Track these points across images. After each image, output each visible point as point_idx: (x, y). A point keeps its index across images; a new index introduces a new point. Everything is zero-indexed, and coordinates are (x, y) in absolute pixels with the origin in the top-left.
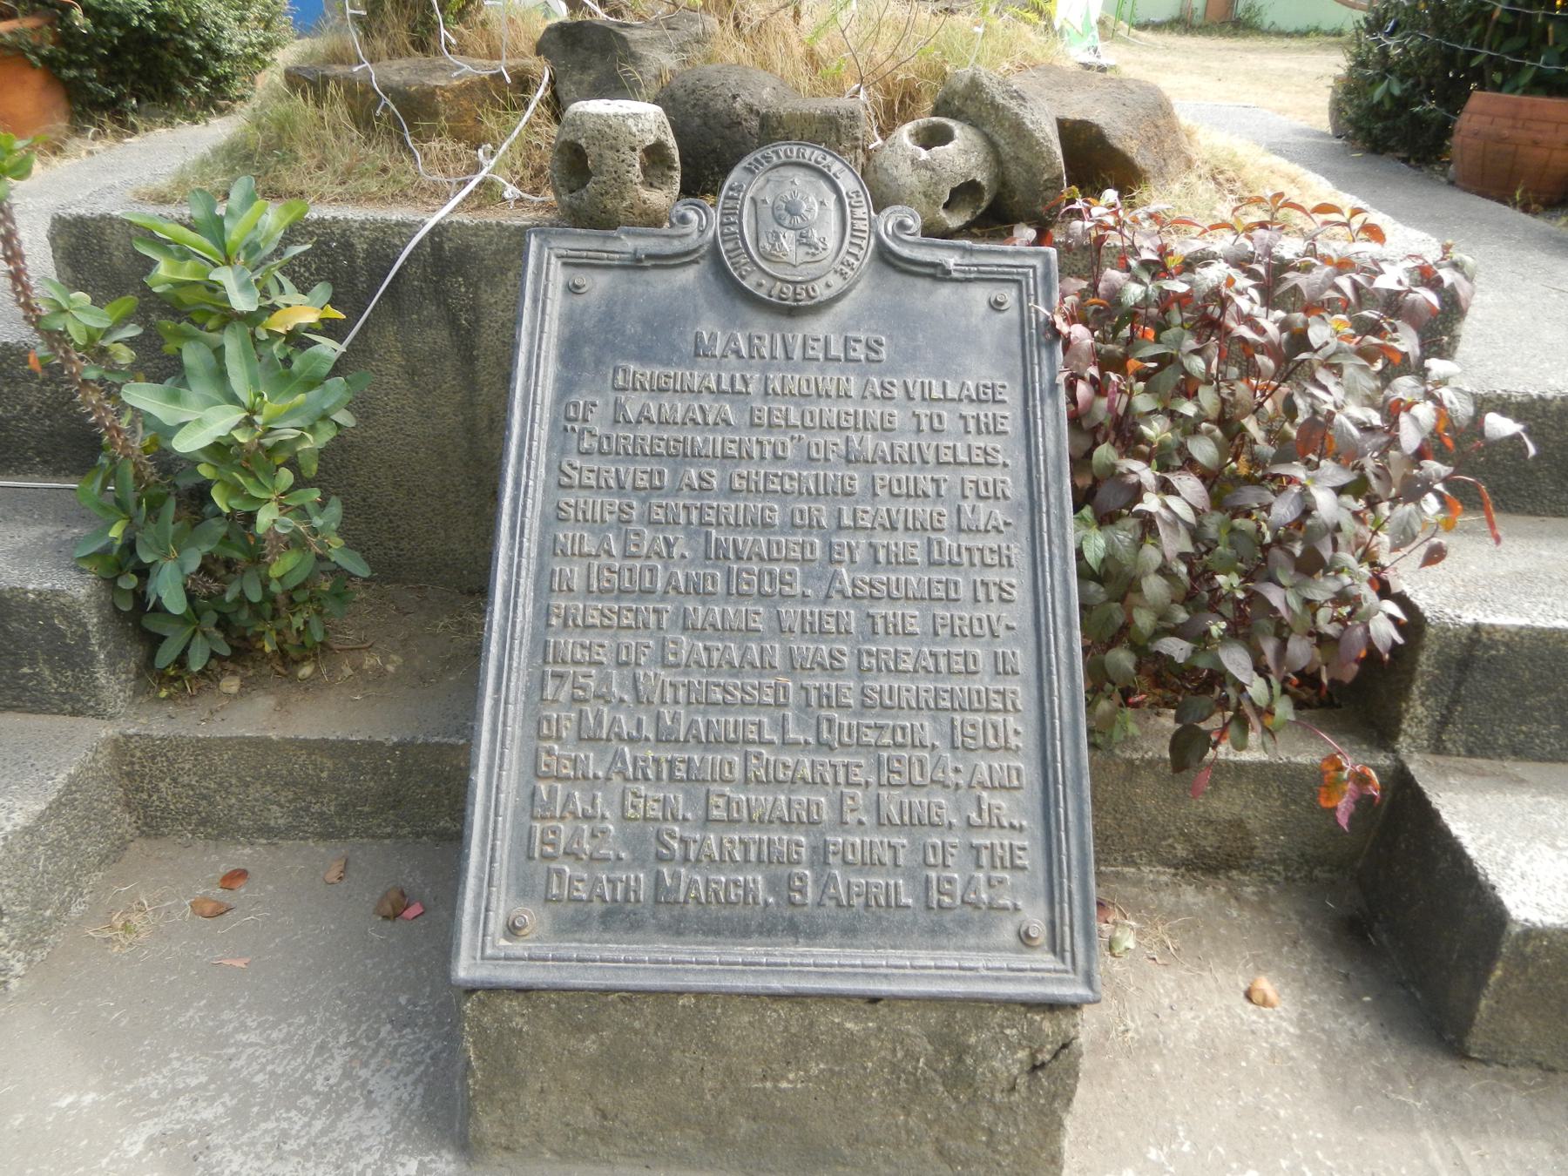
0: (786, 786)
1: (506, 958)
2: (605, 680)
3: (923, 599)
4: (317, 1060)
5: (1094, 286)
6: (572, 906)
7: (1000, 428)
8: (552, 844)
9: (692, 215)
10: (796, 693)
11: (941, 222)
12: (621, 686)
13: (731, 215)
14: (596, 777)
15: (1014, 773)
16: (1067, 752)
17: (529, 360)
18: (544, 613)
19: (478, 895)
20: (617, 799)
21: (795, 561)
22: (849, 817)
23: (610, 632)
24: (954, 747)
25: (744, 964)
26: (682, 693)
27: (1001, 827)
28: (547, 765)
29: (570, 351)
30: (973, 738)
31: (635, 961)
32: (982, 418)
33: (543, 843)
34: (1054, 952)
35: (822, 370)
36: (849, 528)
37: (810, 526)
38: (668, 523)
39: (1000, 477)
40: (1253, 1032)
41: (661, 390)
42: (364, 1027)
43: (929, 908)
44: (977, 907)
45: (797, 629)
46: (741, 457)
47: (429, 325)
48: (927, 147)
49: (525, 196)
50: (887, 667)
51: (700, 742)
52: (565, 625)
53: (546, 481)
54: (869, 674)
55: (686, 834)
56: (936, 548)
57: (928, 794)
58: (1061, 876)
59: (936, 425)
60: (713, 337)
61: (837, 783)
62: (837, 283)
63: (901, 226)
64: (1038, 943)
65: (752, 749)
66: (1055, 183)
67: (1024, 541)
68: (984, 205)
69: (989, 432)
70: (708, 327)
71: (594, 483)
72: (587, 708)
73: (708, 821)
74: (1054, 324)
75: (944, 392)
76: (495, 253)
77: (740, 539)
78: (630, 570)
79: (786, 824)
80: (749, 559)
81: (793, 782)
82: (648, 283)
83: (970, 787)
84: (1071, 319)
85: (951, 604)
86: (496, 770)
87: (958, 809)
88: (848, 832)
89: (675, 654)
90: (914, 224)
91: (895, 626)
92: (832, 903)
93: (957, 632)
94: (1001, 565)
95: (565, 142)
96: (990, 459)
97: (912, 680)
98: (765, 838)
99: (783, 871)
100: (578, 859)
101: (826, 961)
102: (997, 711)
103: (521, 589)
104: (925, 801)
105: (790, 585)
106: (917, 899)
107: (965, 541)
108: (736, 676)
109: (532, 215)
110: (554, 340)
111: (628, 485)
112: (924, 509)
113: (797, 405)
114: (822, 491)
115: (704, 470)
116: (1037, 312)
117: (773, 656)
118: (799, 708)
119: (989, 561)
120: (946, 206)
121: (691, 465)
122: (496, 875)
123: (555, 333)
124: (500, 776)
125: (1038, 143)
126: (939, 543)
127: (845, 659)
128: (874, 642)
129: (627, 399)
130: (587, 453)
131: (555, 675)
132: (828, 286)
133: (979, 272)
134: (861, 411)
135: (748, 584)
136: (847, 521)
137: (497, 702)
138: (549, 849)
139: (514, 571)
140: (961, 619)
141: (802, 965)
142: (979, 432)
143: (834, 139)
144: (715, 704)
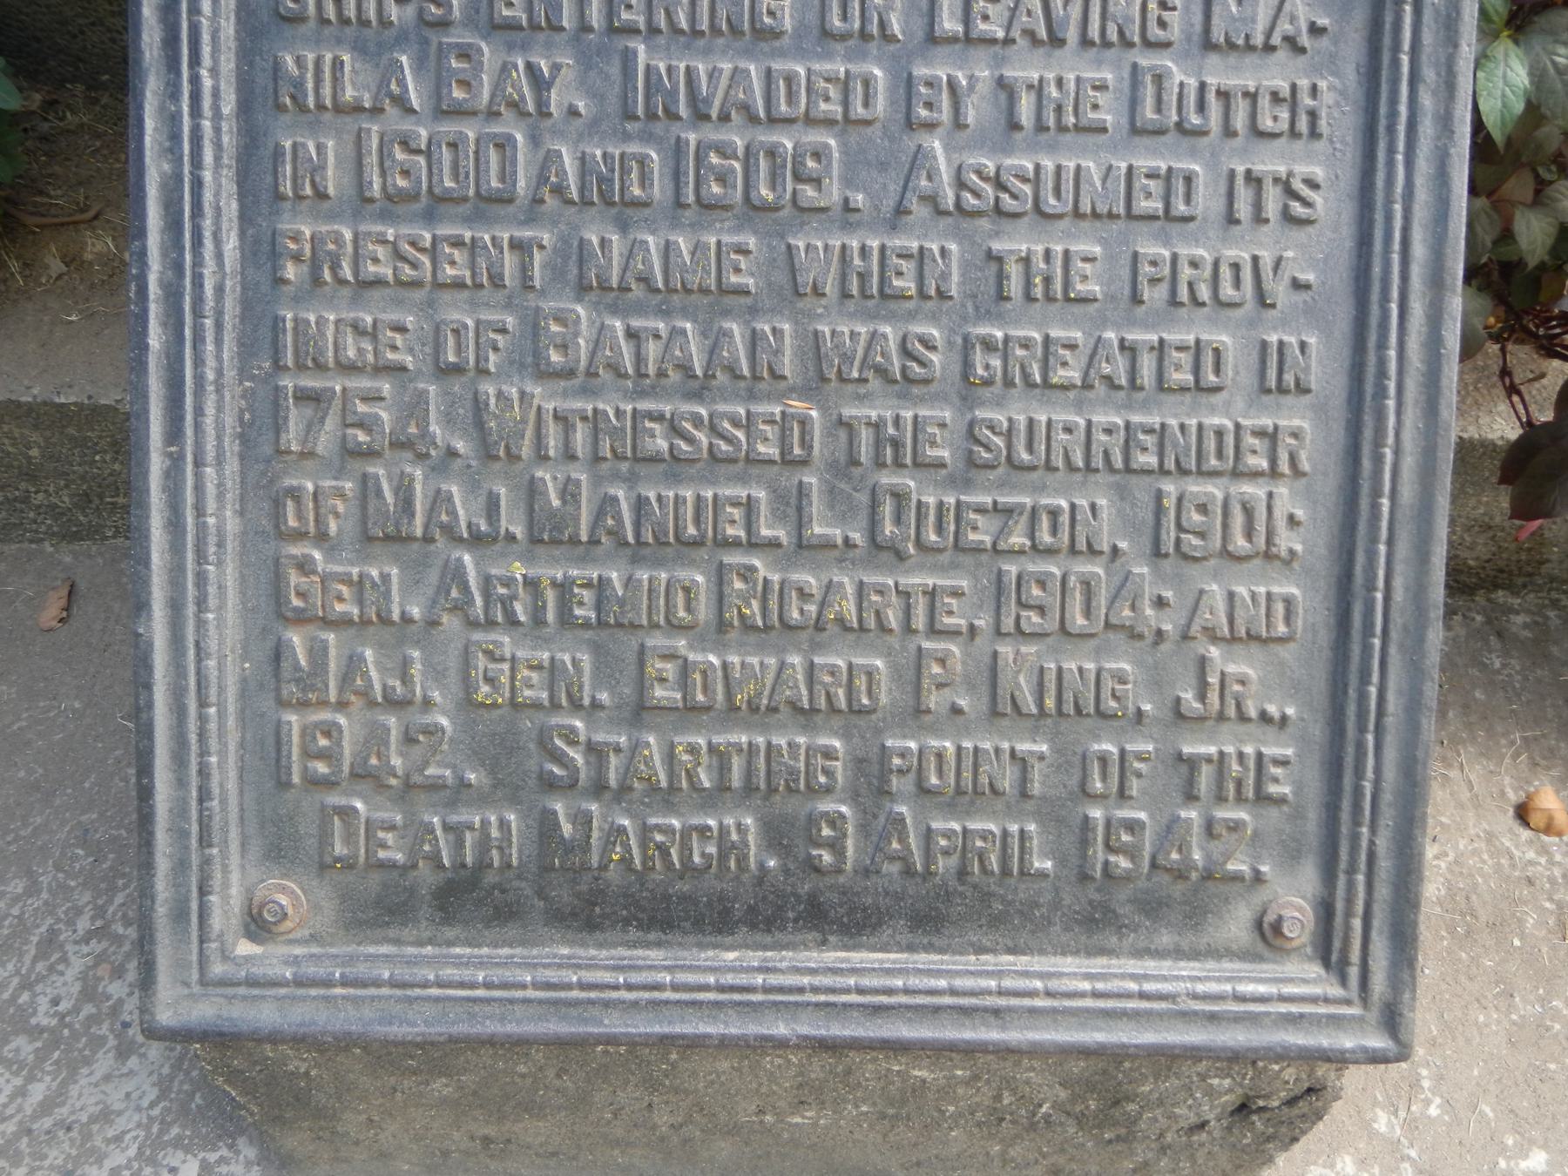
0: (804, 636)
1: (252, 982)
2: (415, 408)
3: (1111, 216)
4: (41, 967)
6: (375, 879)
8: (322, 755)
10: (829, 434)
12: (449, 420)
14: (406, 619)
15: (1279, 608)
16: (1399, 567)
18: (263, 251)
19: (181, 866)
20: (453, 662)
21: (829, 122)
22: (933, 700)
23: (418, 295)
24: (1157, 553)
25: (722, 989)
26: (580, 435)
27: (1243, 718)
28: (300, 594)
30: (1202, 535)
33: (307, 754)
34: (1326, 963)
36: (953, 40)
38: (535, 27)
40: (1530, 882)
42: (119, 899)
43: (1084, 878)
45: (830, 288)
50: (1026, 376)
52: (317, 281)
54: (986, 393)
55: (599, 737)
56: (1149, 91)
61: (908, 629)
64: (1295, 944)
65: (734, 558)
67: (1351, 76)
72: (378, 470)
73: (640, 711)
78: (453, 146)
79: (805, 715)
80: (725, 118)
85: (1175, 228)
86: (191, 609)
87: (1156, 681)
88: (935, 730)
89: (563, 347)
91: (1047, 280)
93: (1183, 293)
94: (1294, 133)
97: (1079, 406)
100: (382, 787)
102: (1255, 475)
103: (208, 196)
104: (1090, 666)
105: (817, 182)
106: (1061, 862)
107: (1219, 74)
108: (697, 396)
117: (778, 352)
119: (1267, 124)
124: (201, 624)
126: (1159, 79)
127: (934, 358)
131: (303, 396)
135: (722, 179)
137: (176, 461)
138: (322, 768)
140: (1194, 264)
141: (833, 991)
144: (655, 459)
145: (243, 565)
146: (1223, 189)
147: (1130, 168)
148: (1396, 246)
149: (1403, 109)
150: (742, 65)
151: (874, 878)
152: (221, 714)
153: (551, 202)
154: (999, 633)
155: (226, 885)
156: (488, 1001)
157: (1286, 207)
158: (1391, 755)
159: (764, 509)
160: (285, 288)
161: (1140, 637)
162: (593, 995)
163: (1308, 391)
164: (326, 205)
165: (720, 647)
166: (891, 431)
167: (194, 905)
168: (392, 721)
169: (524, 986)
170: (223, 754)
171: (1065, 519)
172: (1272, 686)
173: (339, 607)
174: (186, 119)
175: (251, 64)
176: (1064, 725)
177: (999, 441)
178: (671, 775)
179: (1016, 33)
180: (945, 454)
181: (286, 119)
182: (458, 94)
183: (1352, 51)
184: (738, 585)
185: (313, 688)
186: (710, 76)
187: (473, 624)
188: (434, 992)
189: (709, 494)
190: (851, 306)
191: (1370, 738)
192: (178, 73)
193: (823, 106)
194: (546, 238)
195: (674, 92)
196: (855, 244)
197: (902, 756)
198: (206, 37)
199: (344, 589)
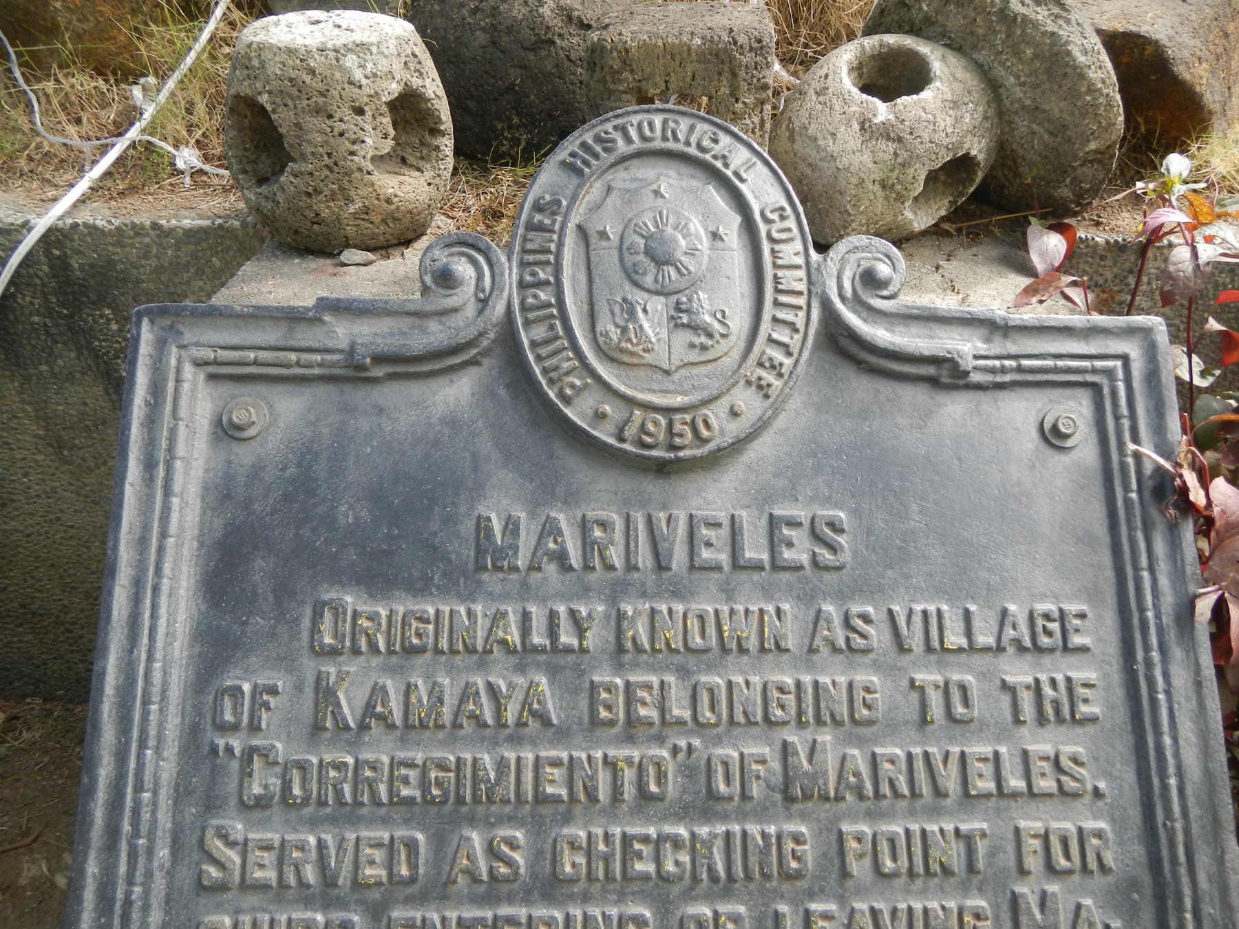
7: (1084, 709)
13: (538, 260)
17: (136, 600)
29: (223, 575)
32: (1048, 691)
35: (729, 593)
39: (1090, 825)
41: (411, 651)
47: (70, 378)
49: (207, 167)
59: (959, 709)
60: (511, 527)
69: (1060, 720)
71: (270, 875)
74: (1184, 490)
75: (969, 633)
76: (159, 270)
95: (237, 96)
111: (344, 879)
113: (683, 672)
114: (739, 872)
115: (504, 832)
116: (1137, 456)
121: (472, 821)
123: (192, 531)
129: (341, 677)
132: (734, 414)
133: (1020, 369)
142: (1041, 719)
143: (725, 90)
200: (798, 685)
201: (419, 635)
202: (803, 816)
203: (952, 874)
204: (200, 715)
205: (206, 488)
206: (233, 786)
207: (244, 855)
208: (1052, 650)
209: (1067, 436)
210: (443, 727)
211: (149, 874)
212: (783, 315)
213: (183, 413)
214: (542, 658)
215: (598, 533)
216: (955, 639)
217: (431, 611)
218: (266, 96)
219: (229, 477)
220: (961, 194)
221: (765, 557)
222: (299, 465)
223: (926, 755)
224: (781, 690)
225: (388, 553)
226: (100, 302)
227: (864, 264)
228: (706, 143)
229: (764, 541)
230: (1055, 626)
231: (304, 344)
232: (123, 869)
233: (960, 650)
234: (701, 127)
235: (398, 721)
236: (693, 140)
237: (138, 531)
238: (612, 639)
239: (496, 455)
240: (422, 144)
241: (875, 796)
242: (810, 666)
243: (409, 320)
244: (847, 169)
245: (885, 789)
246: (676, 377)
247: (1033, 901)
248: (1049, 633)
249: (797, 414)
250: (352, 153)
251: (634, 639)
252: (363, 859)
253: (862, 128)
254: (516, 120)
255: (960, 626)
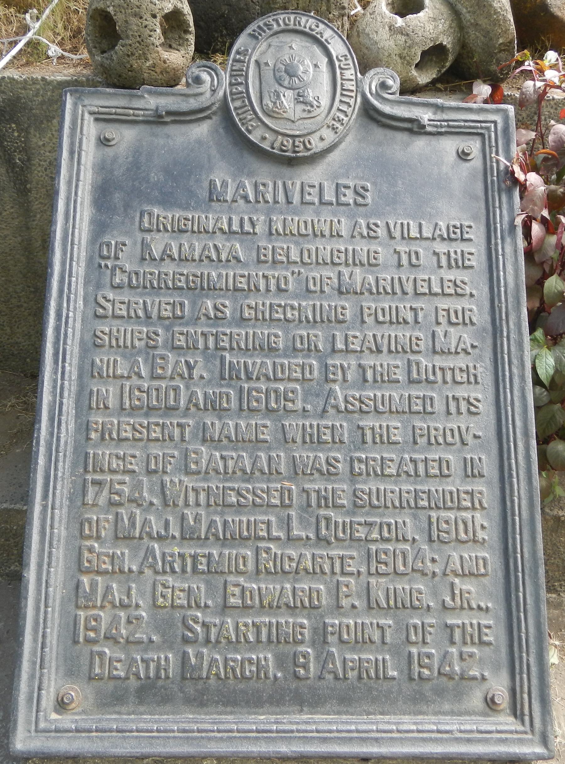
0: (291, 576)
1: (57, 731)
2: (138, 486)
3: (403, 412)
5: (542, 137)
6: (111, 685)
7: (467, 263)
8: (94, 629)
9: (205, 77)
10: (299, 495)
11: (412, 80)
12: (151, 491)
13: (239, 76)
14: (130, 571)
15: (481, 562)
16: (525, 544)
17: (67, 205)
18: (84, 428)
19: (32, 677)
20: (149, 589)
21: (297, 380)
22: (344, 602)
23: (141, 444)
24: (431, 540)
25: (258, 731)
26: (202, 497)
27: (471, 608)
28: (88, 561)
30: (447, 533)
31: (165, 731)
32: (452, 255)
33: (87, 629)
34: (515, 716)
35: (318, 213)
36: (342, 351)
37: (309, 350)
38: (188, 348)
39: (467, 306)
43: (411, 679)
44: (451, 678)
45: (299, 439)
46: (250, 290)
48: (402, 15)
49: (66, 54)
50: (375, 472)
51: (218, 539)
52: (103, 438)
53: (84, 312)
54: (360, 478)
55: (207, 620)
56: (414, 368)
57: (410, 581)
58: (521, 651)
59: (414, 261)
60: (224, 184)
61: (333, 573)
62: (329, 137)
63: (383, 86)
64: (501, 707)
65: (262, 544)
66: (507, 48)
68: (448, 64)
69: (458, 267)
70: (220, 175)
71: (125, 313)
72: (122, 510)
73: (225, 608)
74: (513, 173)
75: (420, 232)
76: (43, 103)
77: (250, 362)
78: (157, 390)
79: (292, 609)
80: (258, 379)
81: (297, 572)
82: (168, 136)
83: (445, 574)
84: (526, 169)
85: (427, 417)
86: (45, 567)
87: (435, 594)
88: (344, 615)
89: (197, 463)
90: (394, 84)
92: (330, 677)
94: (469, 382)
95: (96, 10)
96: (459, 291)
97: (396, 483)
98: (274, 621)
99: (289, 649)
100: (117, 642)
101: (326, 727)
102: (466, 509)
103: (65, 408)
104: (407, 587)
105: (293, 401)
106: (401, 672)
107: (439, 361)
108: (248, 481)
109: (72, 71)
110: (88, 188)
111: (154, 315)
112: (404, 334)
113: (297, 243)
114: (318, 319)
115: (219, 301)
116: (498, 162)
117: (279, 464)
118: (301, 508)
119: (459, 379)
120: (417, 66)
121: (207, 297)
122: (47, 659)
124: (48, 572)
125: (496, 13)
126: (418, 364)
127: (339, 465)
128: (364, 450)
130: (119, 287)
131: (94, 482)
132: (322, 139)
133: (449, 126)
134: (350, 248)
135: (257, 401)
136: (340, 345)
137: (45, 507)
138: (92, 634)
139: (58, 392)
140: (436, 429)
141: (306, 731)
142: (450, 267)
143: (324, 8)
144: (231, 506)
145: (67, 549)
146: (445, 402)
147: (409, 395)
148: (510, 422)
149: (507, 374)
150: (265, 360)
151: (323, 681)
152: (53, 611)
153: (193, 409)
154: (369, 574)
155: (49, 687)
156: (158, 738)
157: (469, 409)
158: (531, 621)
159: (274, 525)
160: (91, 442)
161: (426, 575)
162: (203, 735)
163: (483, 476)
164: (108, 411)
165: (257, 581)
166: (323, 493)
167: (36, 695)
168: (122, 614)
169: (173, 731)
170: (52, 629)
171: (393, 527)
172: (481, 594)
173: (104, 566)
174: (59, 381)
175: (83, 362)
176: (398, 612)
177: (366, 497)
178: (237, 636)
179: (364, 349)
180: (345, 502)
181: (95, 380)
182: (160, 371)
183: (488, 355)
184: (264, 555)
185: (91, 600)
186: (253, 364)
187: (156, 572)
188: (135, 734)
189: (252, 519)
190: (307, 446)
191: (522, 615)
192: (58, 365)
193: (294, 374)
194: (191, 422)
195: (239, 371)
196: (308, 424)
197: (332, 626)
198: (68, 352)
199: (106, 559)
200: (346, 250)
201: (185, 225)
202: (346, 300)
203: (408, 323)
204: (94, 252)
205: (94, 165)
206: (108, 280)
207: (113, 305)
208: (456, 240)
209: (468, 154)
210: (195, 260)
211: (75, 308)
212: (344, 99)
213: (85, 132)
214: (238, 236)
215: (261, 188)
216: (414, 233)
217: (190, 217)
218: (111, 8)
219: (103, 161)
220: (443, 67)
221: (334, 200)
222: (133, 157)
223: (400, 278)
224: (339, 251)
225: (172, 193)
226: (11, 120)
227: (381, 80)
228: (313, 27)
229: (334, 194)
230: (458, 231)
231: (136, 106)
232: (65, 305)
233: (416, 238)
234: (311, 20)
235: (176, 257)
236: (308, 26)
237: (67, 178)
238: (267, 230)
239: (218, 156)
240: (180, 38)
241: (378, 292)
242: (352, 243)
243: (181, 98)
244: (383, 48)
245: (381, 290)
246: (297, 124)
247: (442, 334)
248: (455, 233)
249: (349, 144)
250: (150, 36)
251: (276, 230)
252: (162, 308)
253: (390, 29)
254: (225, 32)
255: (417, 230)
